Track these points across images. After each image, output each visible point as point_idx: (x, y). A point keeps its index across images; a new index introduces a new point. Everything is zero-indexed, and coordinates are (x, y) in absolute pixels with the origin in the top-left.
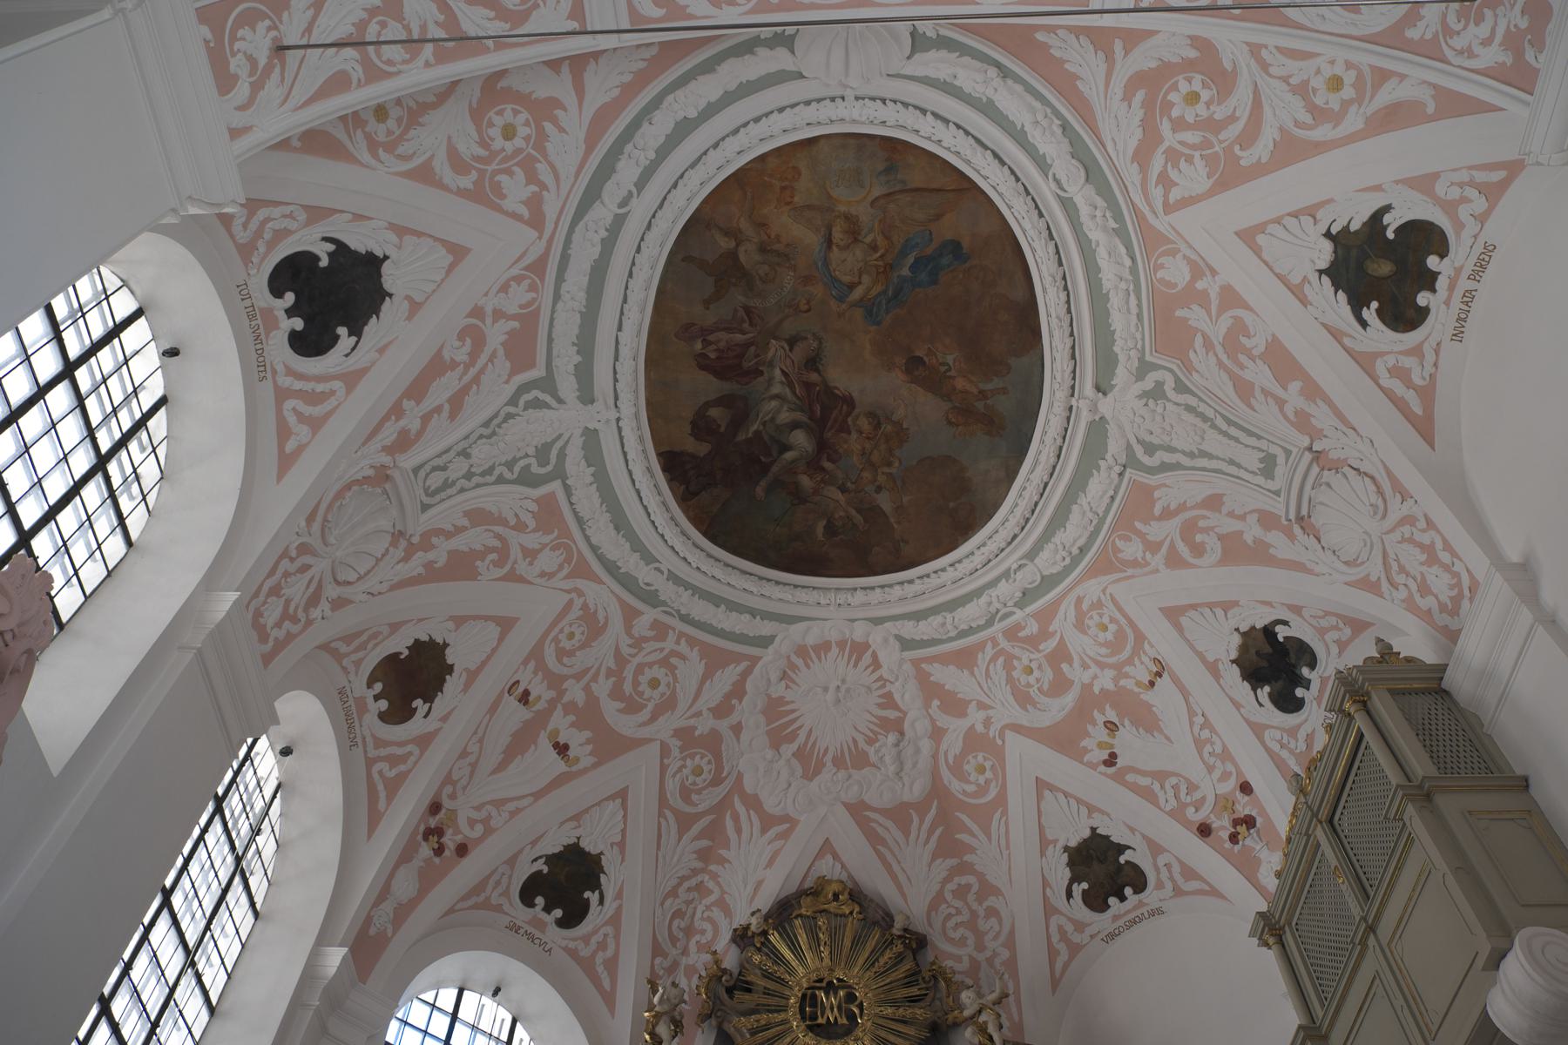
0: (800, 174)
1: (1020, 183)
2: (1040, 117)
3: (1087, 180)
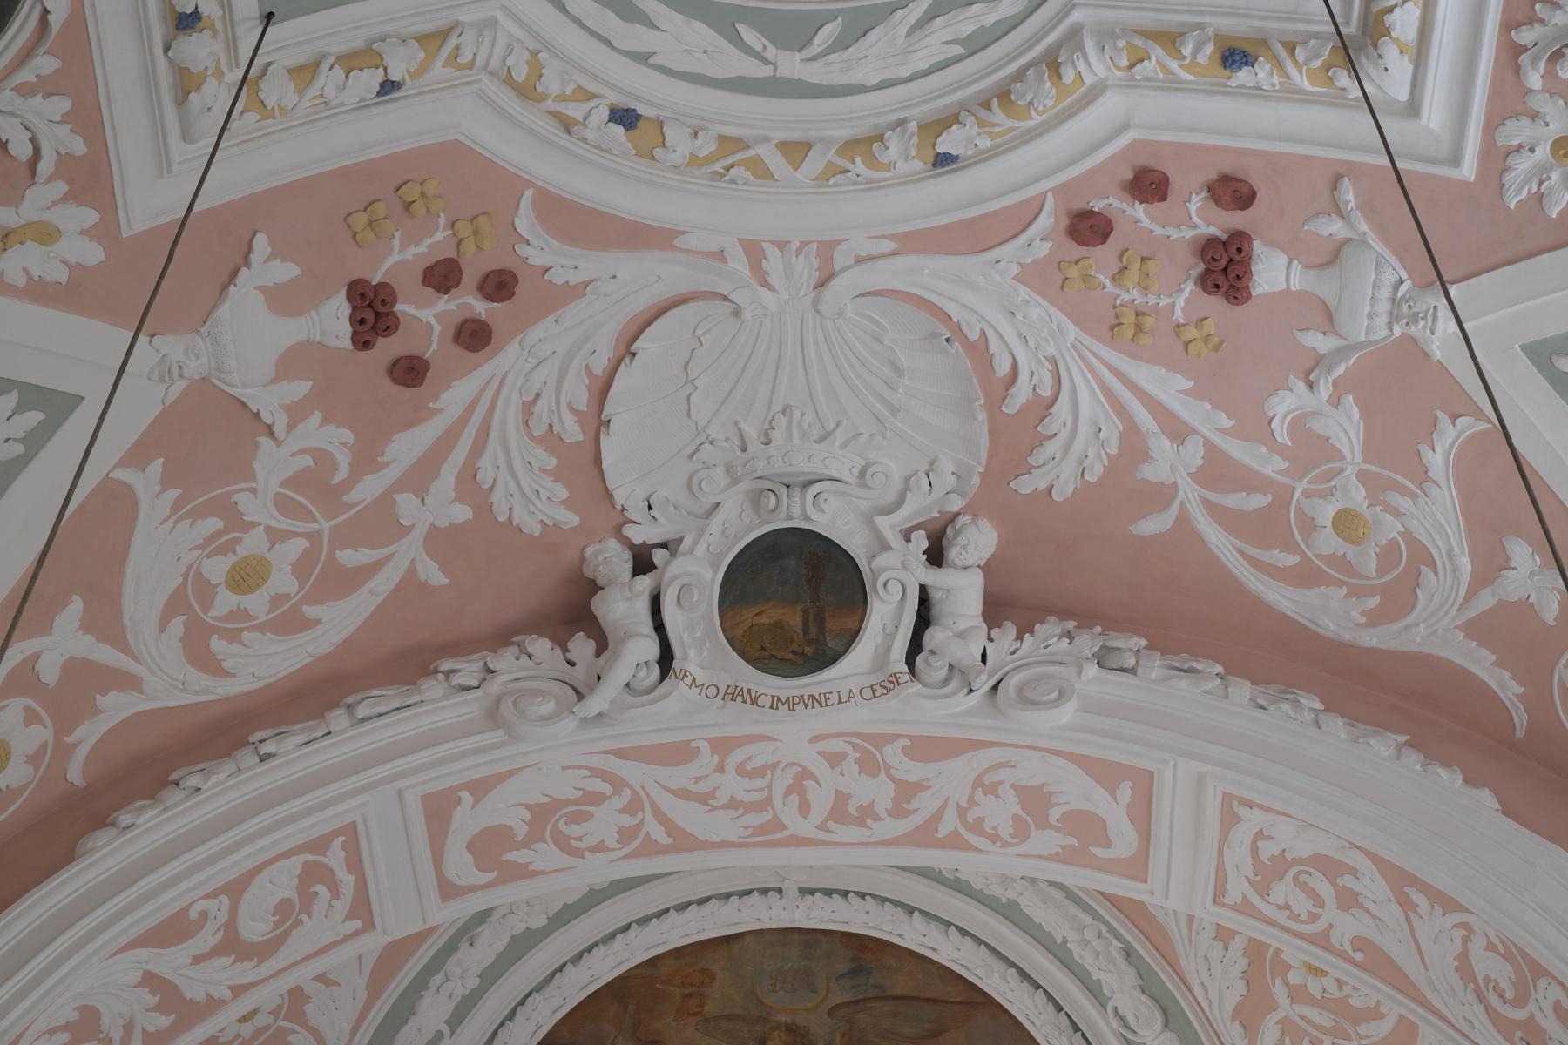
0: (713, 978)
1: (1062, 1013)
2: (1090, 935)
3: (1166, 1024)
